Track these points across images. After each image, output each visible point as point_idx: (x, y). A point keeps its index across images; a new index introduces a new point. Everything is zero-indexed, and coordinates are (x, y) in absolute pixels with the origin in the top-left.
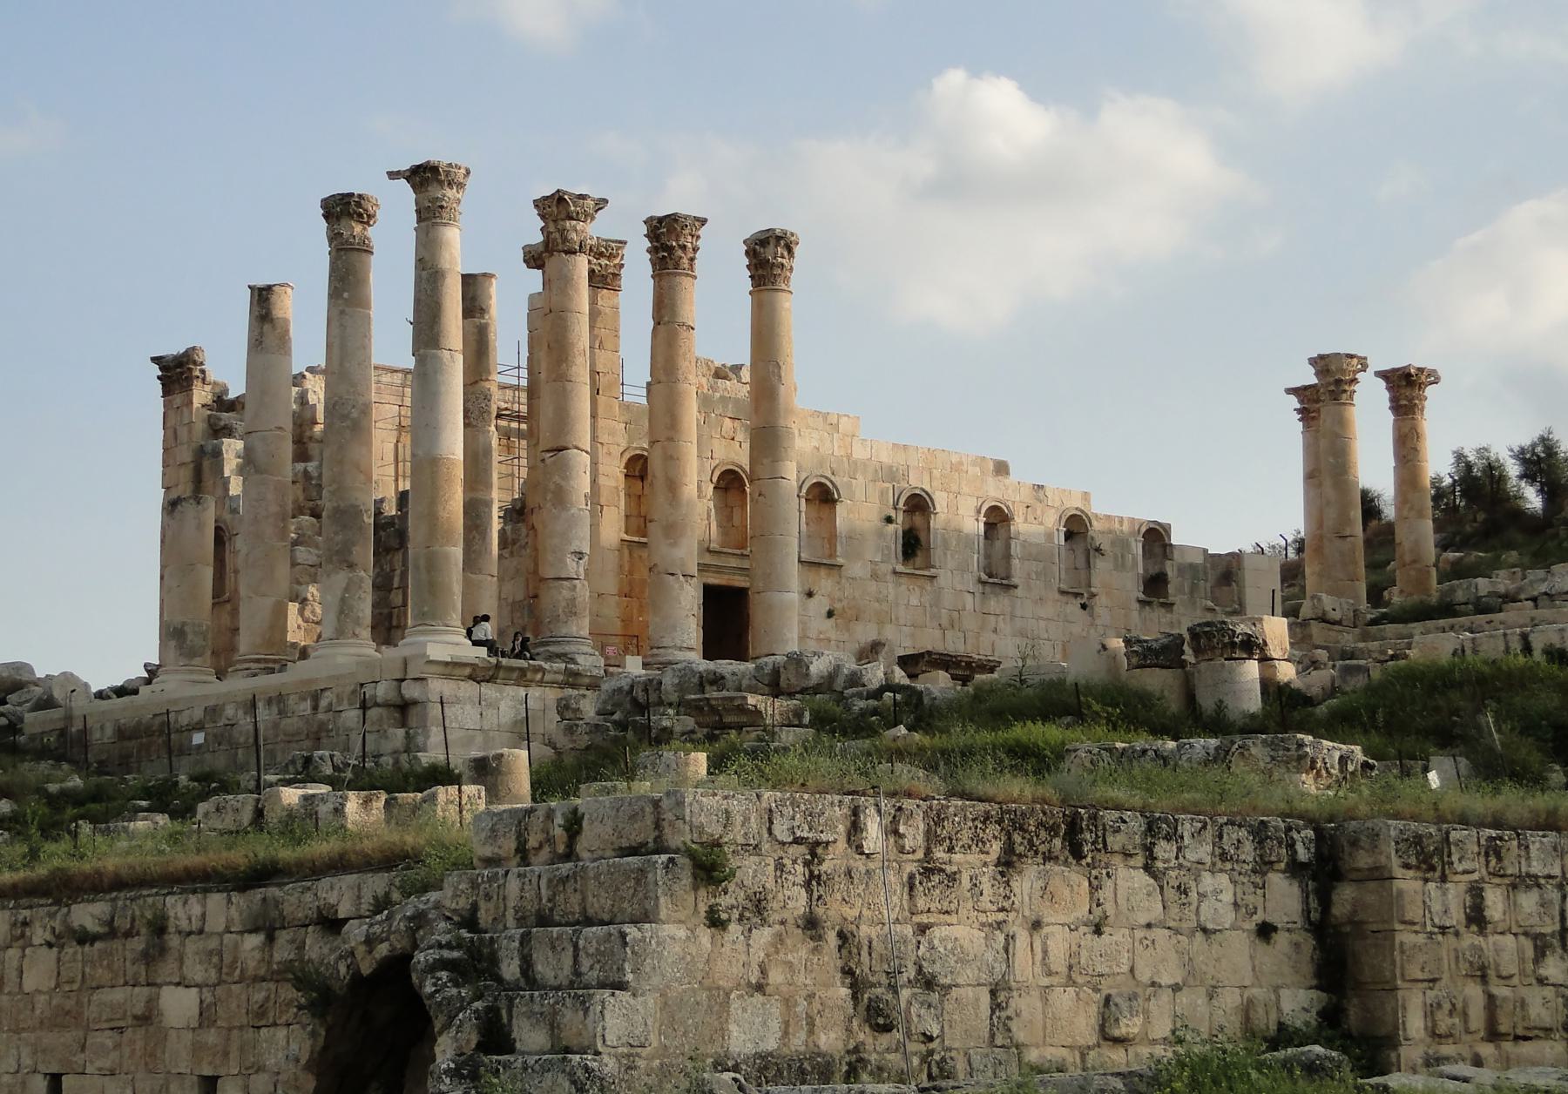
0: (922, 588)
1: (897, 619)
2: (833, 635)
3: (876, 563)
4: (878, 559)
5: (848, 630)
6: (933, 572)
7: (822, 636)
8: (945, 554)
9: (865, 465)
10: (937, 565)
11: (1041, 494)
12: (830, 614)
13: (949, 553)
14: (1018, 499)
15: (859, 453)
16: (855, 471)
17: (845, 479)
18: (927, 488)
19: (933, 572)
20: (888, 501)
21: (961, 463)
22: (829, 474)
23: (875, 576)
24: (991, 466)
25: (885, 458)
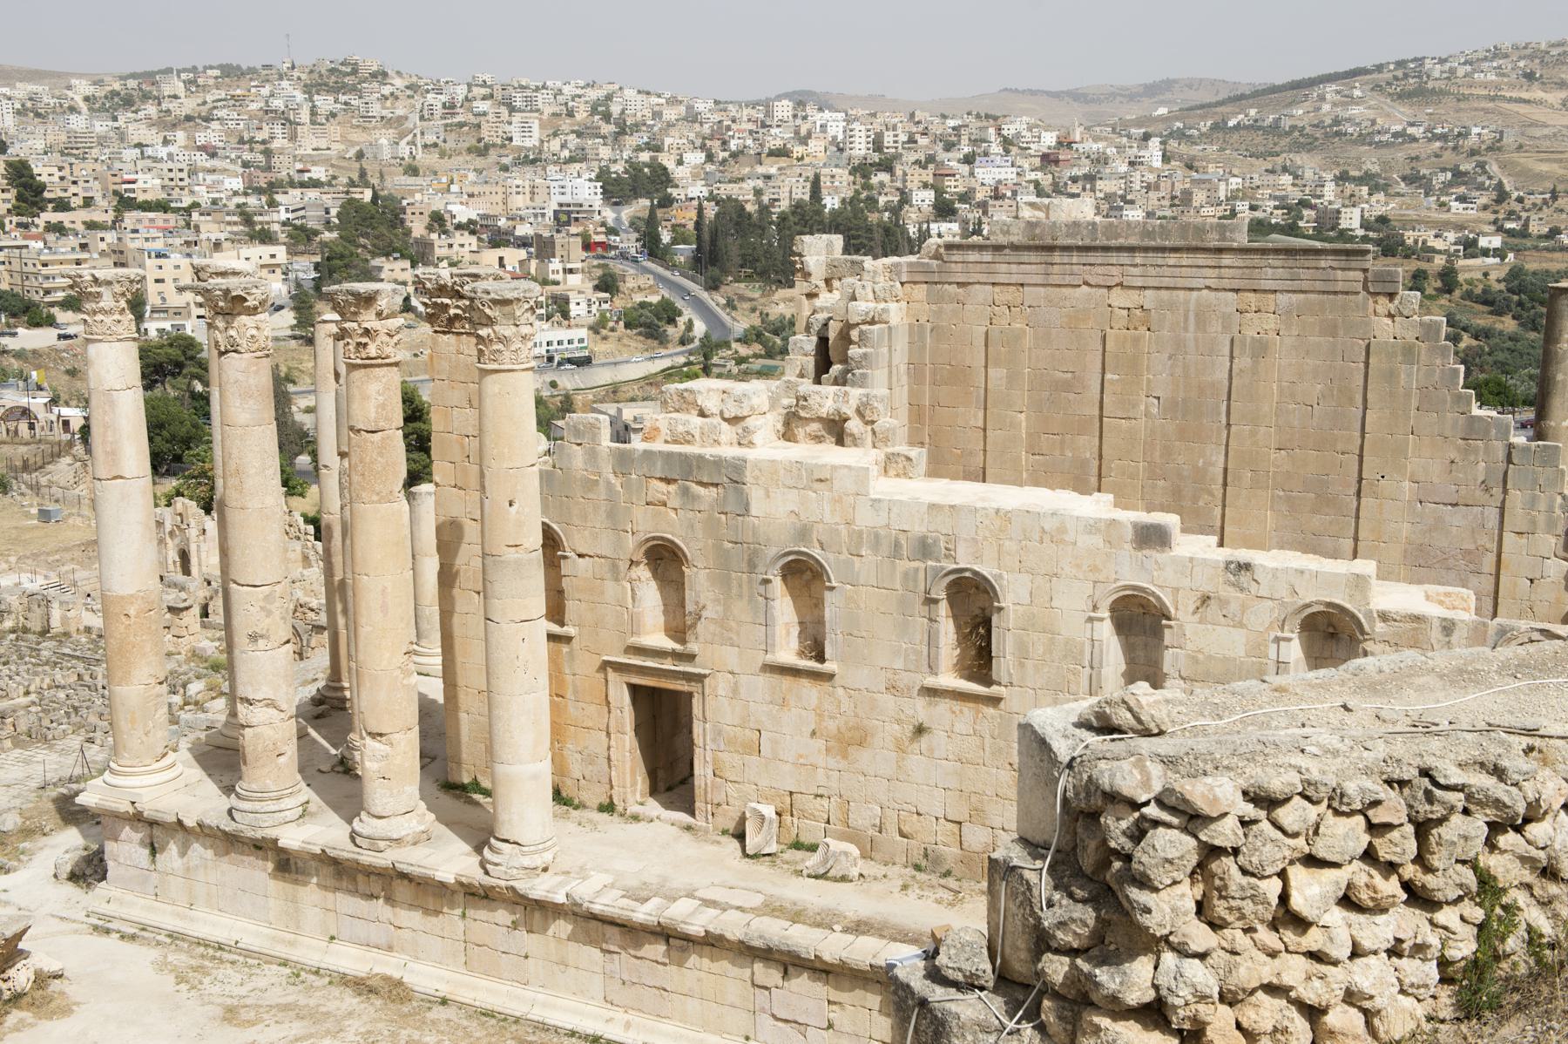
0: (978, 712)
1: (931, 750)
2: (821, 760)
3: (895, 672)
4: (899, 664)
5: (845, 757)
6: (995, 690)
7: (801, 761)
8: (1022, 665)
9: (877, 536)
10: (1004, 681)
11: (1244, 578)
12: (814, 733)
13: (1029, 663)
14: (1186, 582)
15: (866, 519)
16: (859, 544)
17: (842, 557)
18: (985, 570)
19: (995, 690)
20: (916, 587)
21: (1062, 530)
22: (816, 552)
23: (892, 688)
24: (1129, 534)
25: (918, 529)
